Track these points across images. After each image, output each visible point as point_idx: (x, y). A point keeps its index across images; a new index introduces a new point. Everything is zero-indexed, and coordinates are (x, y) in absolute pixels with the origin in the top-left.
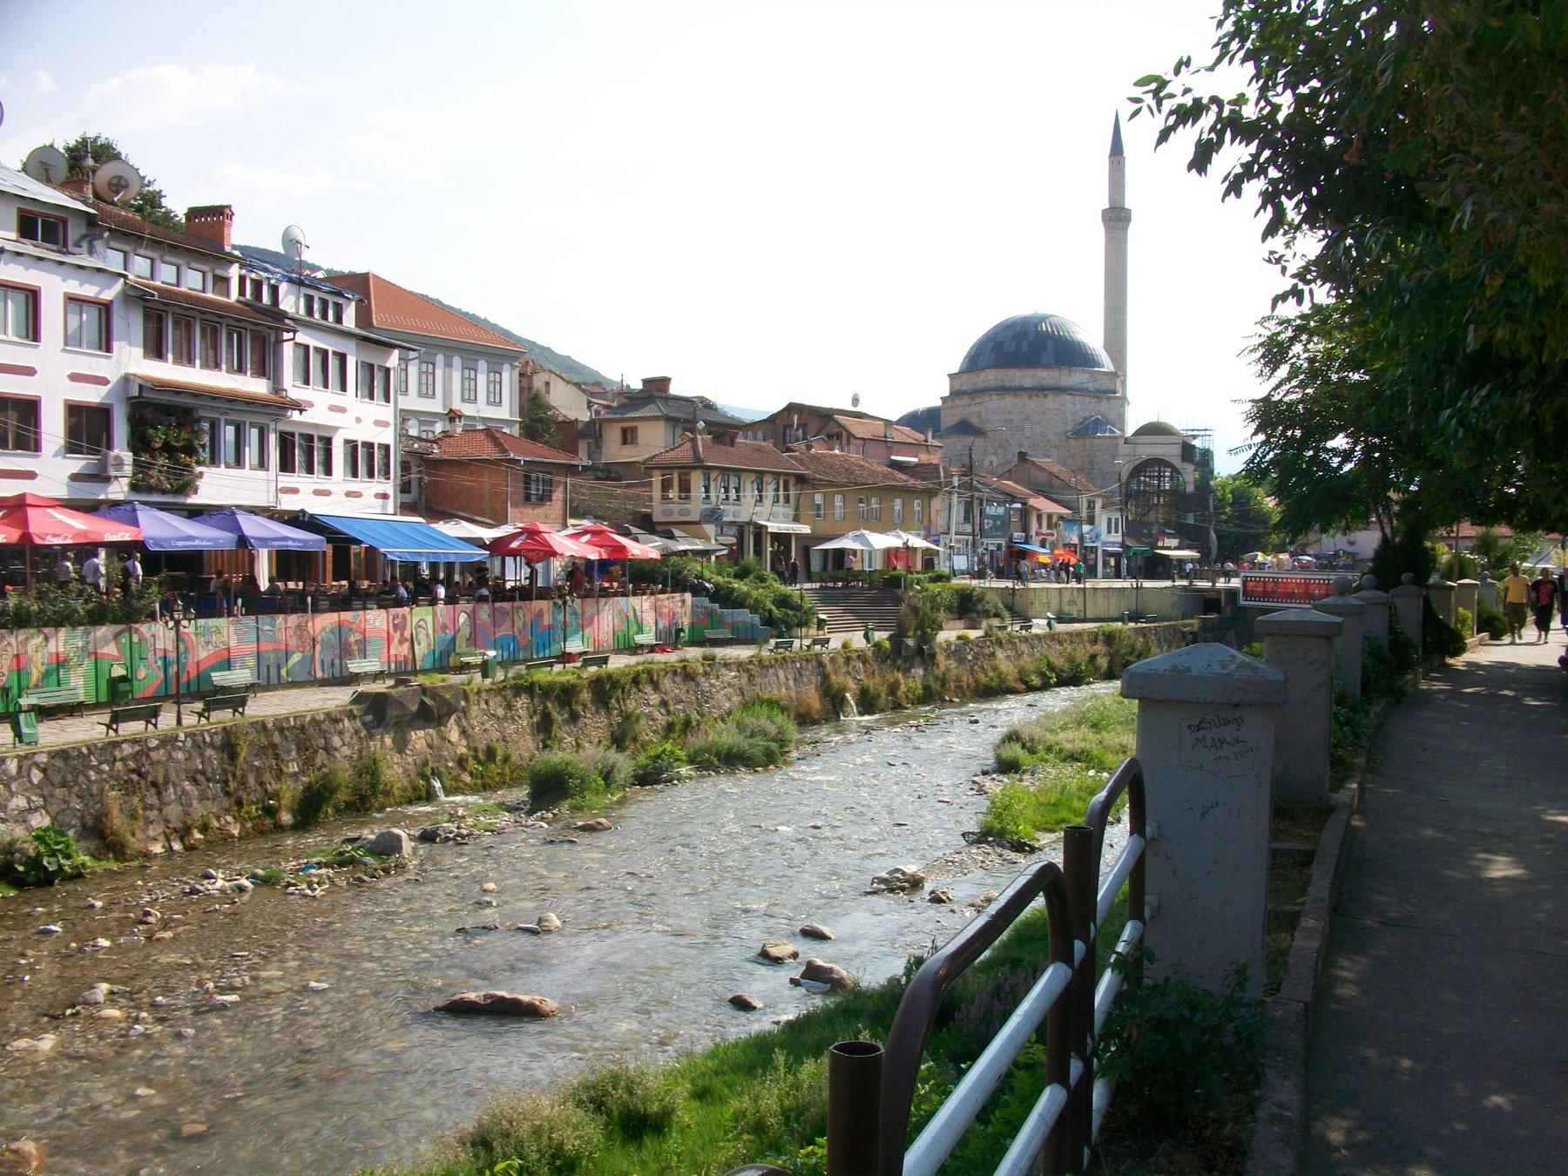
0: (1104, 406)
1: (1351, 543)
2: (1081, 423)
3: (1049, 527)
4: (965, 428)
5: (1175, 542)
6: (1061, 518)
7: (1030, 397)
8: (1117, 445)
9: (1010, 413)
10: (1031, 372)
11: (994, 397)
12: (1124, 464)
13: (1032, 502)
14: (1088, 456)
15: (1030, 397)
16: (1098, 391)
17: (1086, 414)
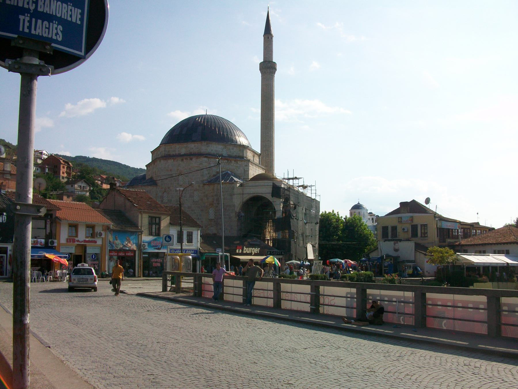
0: (232, 166)
1: (396, 250)
2: (214, 176)
3: (93, 235)
4: (153, 182)
5: (256, 250)
6: (107, 228)
7: (182, 160)
8: (233, 188)
9: (171, 170)
10: (185, 145)
11: (162, 161)
12: (238, 202)
13: (58, 214)
15: (182, 160)
16: (230, 156)
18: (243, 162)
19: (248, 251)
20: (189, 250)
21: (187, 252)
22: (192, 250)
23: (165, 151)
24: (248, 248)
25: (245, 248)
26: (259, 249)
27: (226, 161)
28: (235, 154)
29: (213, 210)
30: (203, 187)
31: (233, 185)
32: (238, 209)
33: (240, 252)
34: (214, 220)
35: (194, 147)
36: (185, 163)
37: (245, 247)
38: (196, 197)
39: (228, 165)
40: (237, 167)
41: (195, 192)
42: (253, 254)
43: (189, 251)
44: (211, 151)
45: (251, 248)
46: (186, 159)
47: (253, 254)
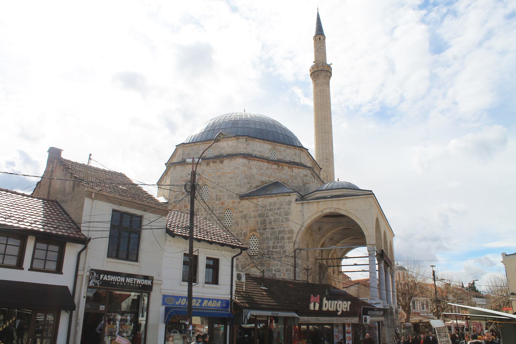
7: (208, 164)
8: (290, 203)
14: (260, 216)
15: (208, 164)
17: (265, 179)
18: (301, 169)
19: (331, 307)
20: (209, 300)
21: (205, 303)
22: (218, 300)
23: (183, 154)
24: (330, 301)
25: (325, 301)
26: (349, 303)
27: (276, 166)
28: (288, 159)
29: (256, 239)
30: (240, 202)
31: (288, 197)
32: (297, 237)
33: (317, 308)
34: (257, 257)
35: (227, 145)
36: (212, 168)
37: (325, 299)
38: (229, 220)
39: (279, 172)
40: (292, 177)
41: (226, 212)
42: (339, 313)
43: (211, 301)
44: (253, 151)
45: (336, 302)
46: (213, 162)
47: (339, 313)
